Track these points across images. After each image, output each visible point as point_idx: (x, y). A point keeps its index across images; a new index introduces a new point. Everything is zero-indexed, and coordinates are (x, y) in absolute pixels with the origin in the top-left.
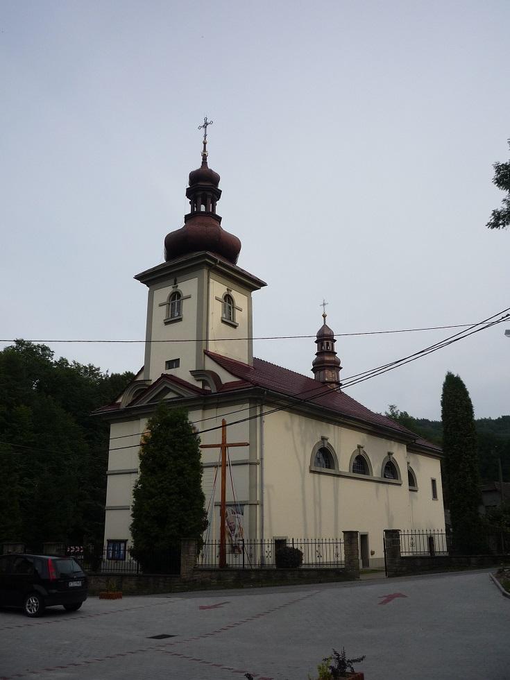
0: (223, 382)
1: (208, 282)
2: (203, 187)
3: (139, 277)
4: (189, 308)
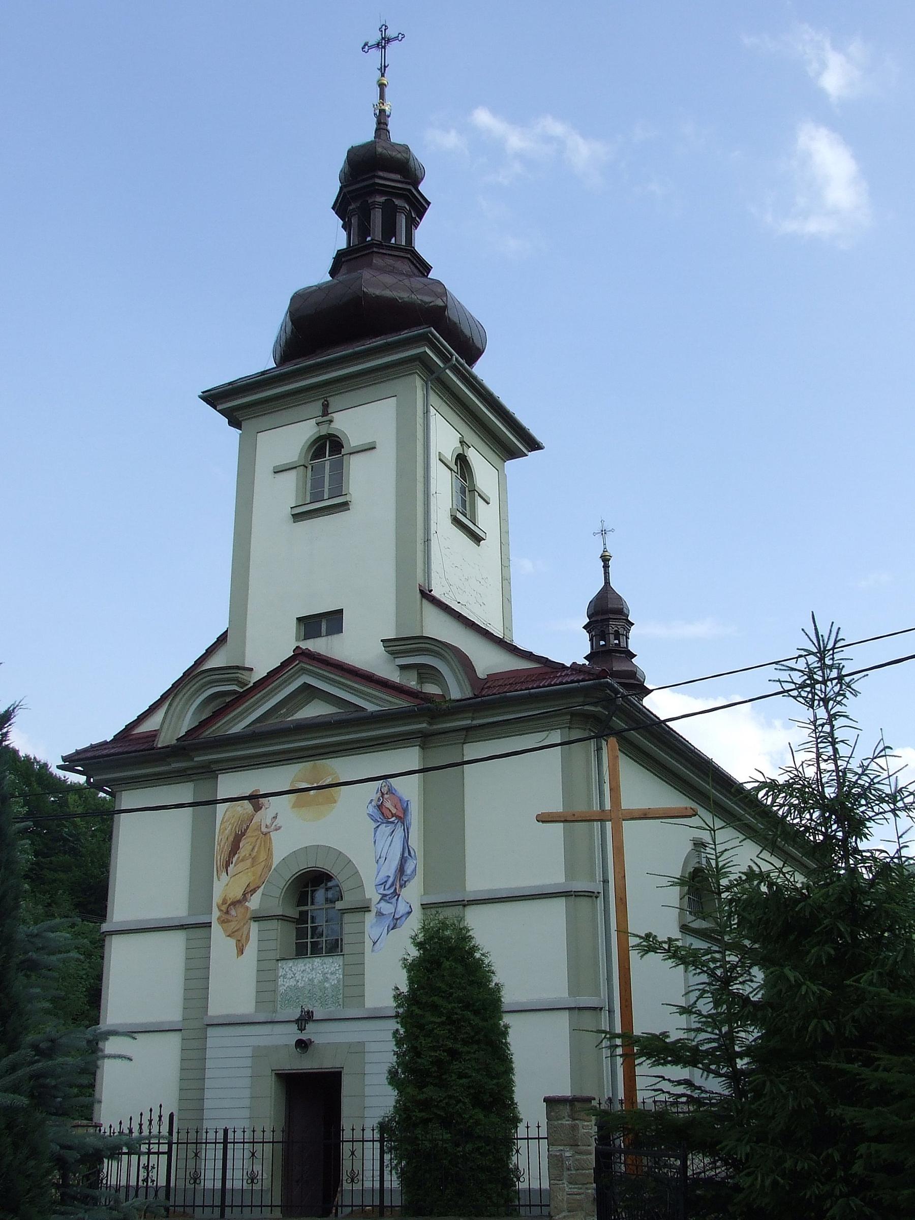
0: (481, 673)
1: (426, 413)
2: (380, 189)
3: (212, 398)
4: (369, 480)
